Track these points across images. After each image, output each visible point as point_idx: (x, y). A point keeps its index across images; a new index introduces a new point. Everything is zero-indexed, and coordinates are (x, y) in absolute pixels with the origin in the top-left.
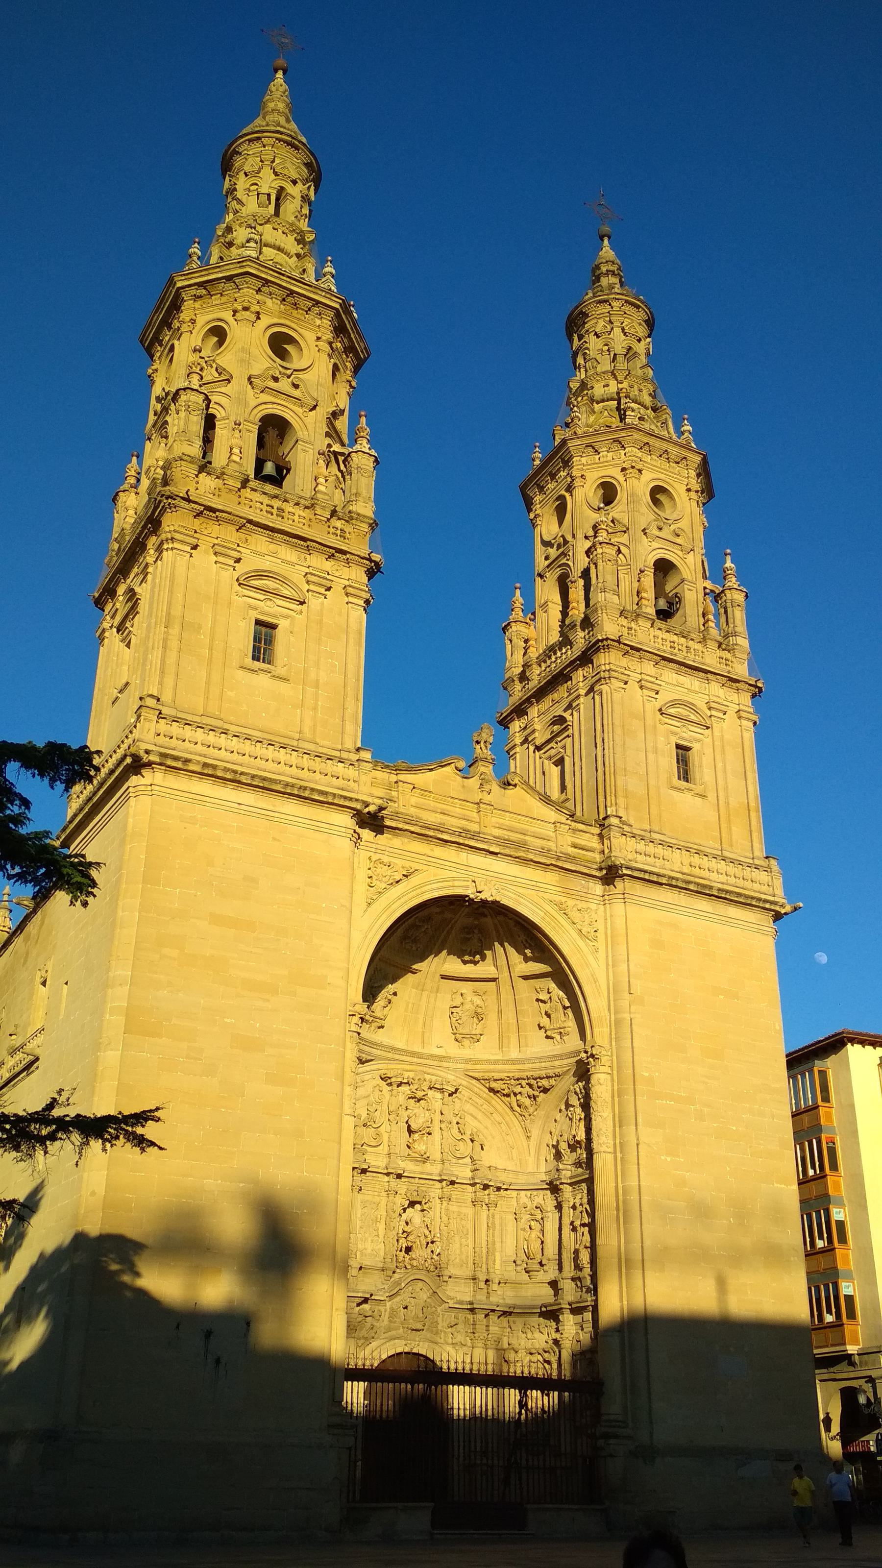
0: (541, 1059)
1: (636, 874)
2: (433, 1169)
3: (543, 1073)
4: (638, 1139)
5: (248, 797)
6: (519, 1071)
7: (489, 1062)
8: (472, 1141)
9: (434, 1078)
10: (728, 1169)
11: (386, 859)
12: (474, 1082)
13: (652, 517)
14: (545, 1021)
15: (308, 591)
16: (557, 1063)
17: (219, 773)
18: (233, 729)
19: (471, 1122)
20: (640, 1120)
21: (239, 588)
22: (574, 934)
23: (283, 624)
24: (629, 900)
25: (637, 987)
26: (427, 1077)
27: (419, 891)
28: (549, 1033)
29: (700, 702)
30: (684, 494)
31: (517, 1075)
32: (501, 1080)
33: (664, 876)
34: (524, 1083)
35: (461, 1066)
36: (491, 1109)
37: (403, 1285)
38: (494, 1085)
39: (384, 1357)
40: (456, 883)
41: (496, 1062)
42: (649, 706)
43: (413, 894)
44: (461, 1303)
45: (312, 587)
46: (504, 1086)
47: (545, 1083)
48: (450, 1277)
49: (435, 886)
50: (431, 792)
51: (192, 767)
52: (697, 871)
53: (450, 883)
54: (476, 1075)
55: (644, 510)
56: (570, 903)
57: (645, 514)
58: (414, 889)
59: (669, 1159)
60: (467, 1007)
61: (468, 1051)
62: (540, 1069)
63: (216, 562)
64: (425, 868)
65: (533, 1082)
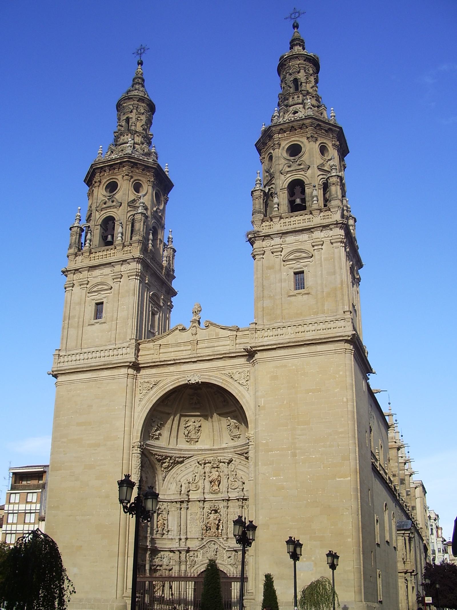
2: (220, 496)
9: (219, 458)
10: (309, 477)
11: (146, 380)
19: (240, 473)
24: (259, 362)
35: (233, 450)
37: (205, 543)
40: (180, 380)
50: (169, 344)
53: (177, 381)
54: (239, 452)
56: (234, 371)
58: (160, 388)
59: (274, 478)
60: (231, 424)
64: (165, 378)
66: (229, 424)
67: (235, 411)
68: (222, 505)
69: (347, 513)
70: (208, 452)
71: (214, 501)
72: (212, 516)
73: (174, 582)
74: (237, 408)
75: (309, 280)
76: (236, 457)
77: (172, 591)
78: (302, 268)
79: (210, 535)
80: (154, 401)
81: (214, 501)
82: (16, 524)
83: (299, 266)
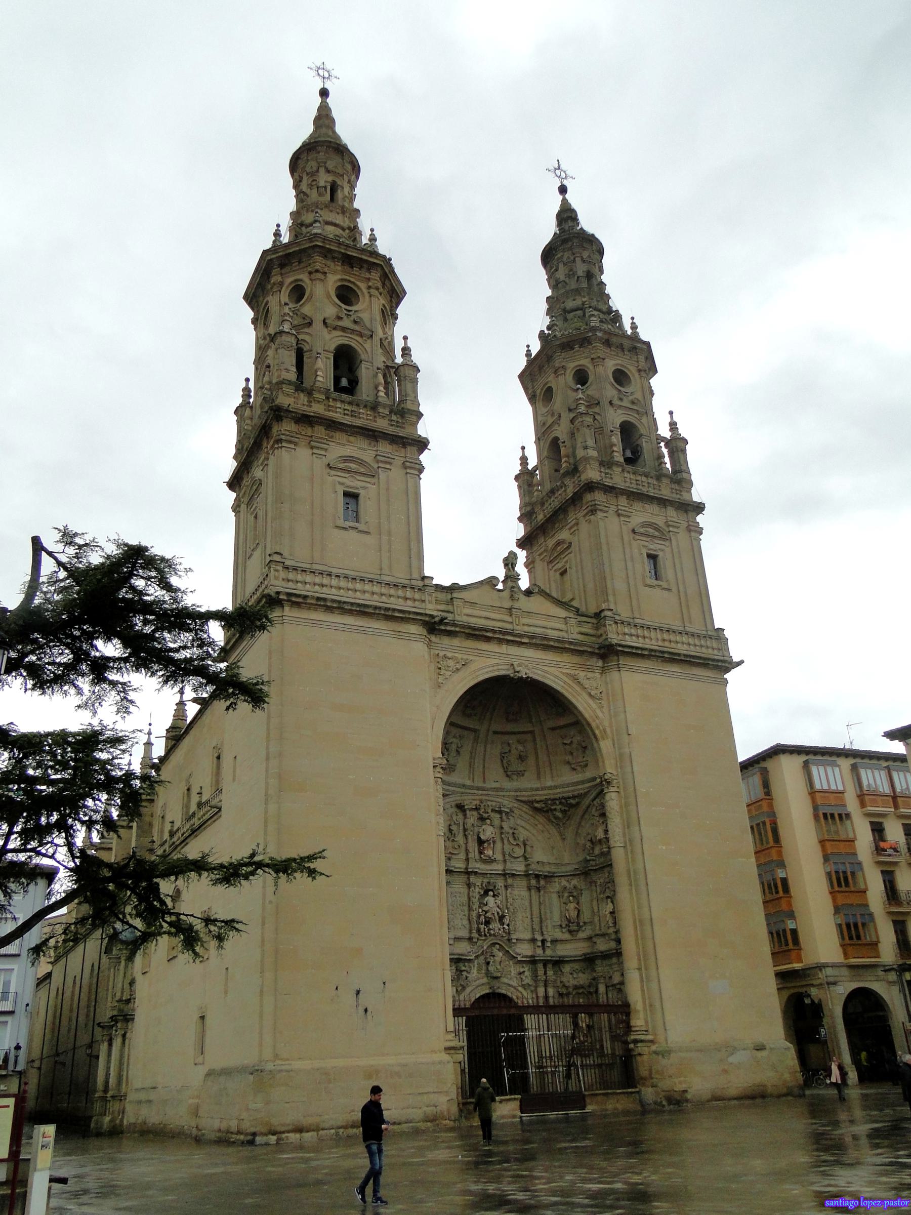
0: (568, 785)
1: (626, 650)
2: (498, 867)
3: (570, 794)
4: (641, 836)
5: (350, 620)
6: (554, 794)
7: (532, 790)
8: (525, 845)
9: (494, 804)
11: (449, 655)
12: (522, 804)
13: (615, 392)
14: (569, 758)
15: (378, 467)
16: (580, 787)
17: (329, 604)
18: (334, 571)
20: (642, 823)
21: (329, 470)
22: (586, 697)
23: (362, 493)
25: (633, 730)
26: (489, 803)
28: (573, 766)
29: (660, 521)
30: (637, 375)
31: (552, 797)
32: (541, 801)
33: (646, 649)
34: (557, 802)
36: (537, 823)
38: (536, 805)
41: (537, 789)
42: (624, 527)
44: (526, 957)
45: (381, 465)
46: (544, 805)
47: (573, 801)
48: (517, 940)
49: (486, 670)
51: (309, 601)
52: (667, 644)
53: (496, 668)
55: (609, 387)
57: (610, 392)
59: (664, 848)
60: (514, 751)
61: (515, 784)
62: (569, 792)
63: (313, 453)
65: (563, 801)
67: (532, 732)
68: (500, 883)
70: (472, 791)
71: (488, 875)
76: (516, 805)
79: (494, 935)
81: (488, 875)
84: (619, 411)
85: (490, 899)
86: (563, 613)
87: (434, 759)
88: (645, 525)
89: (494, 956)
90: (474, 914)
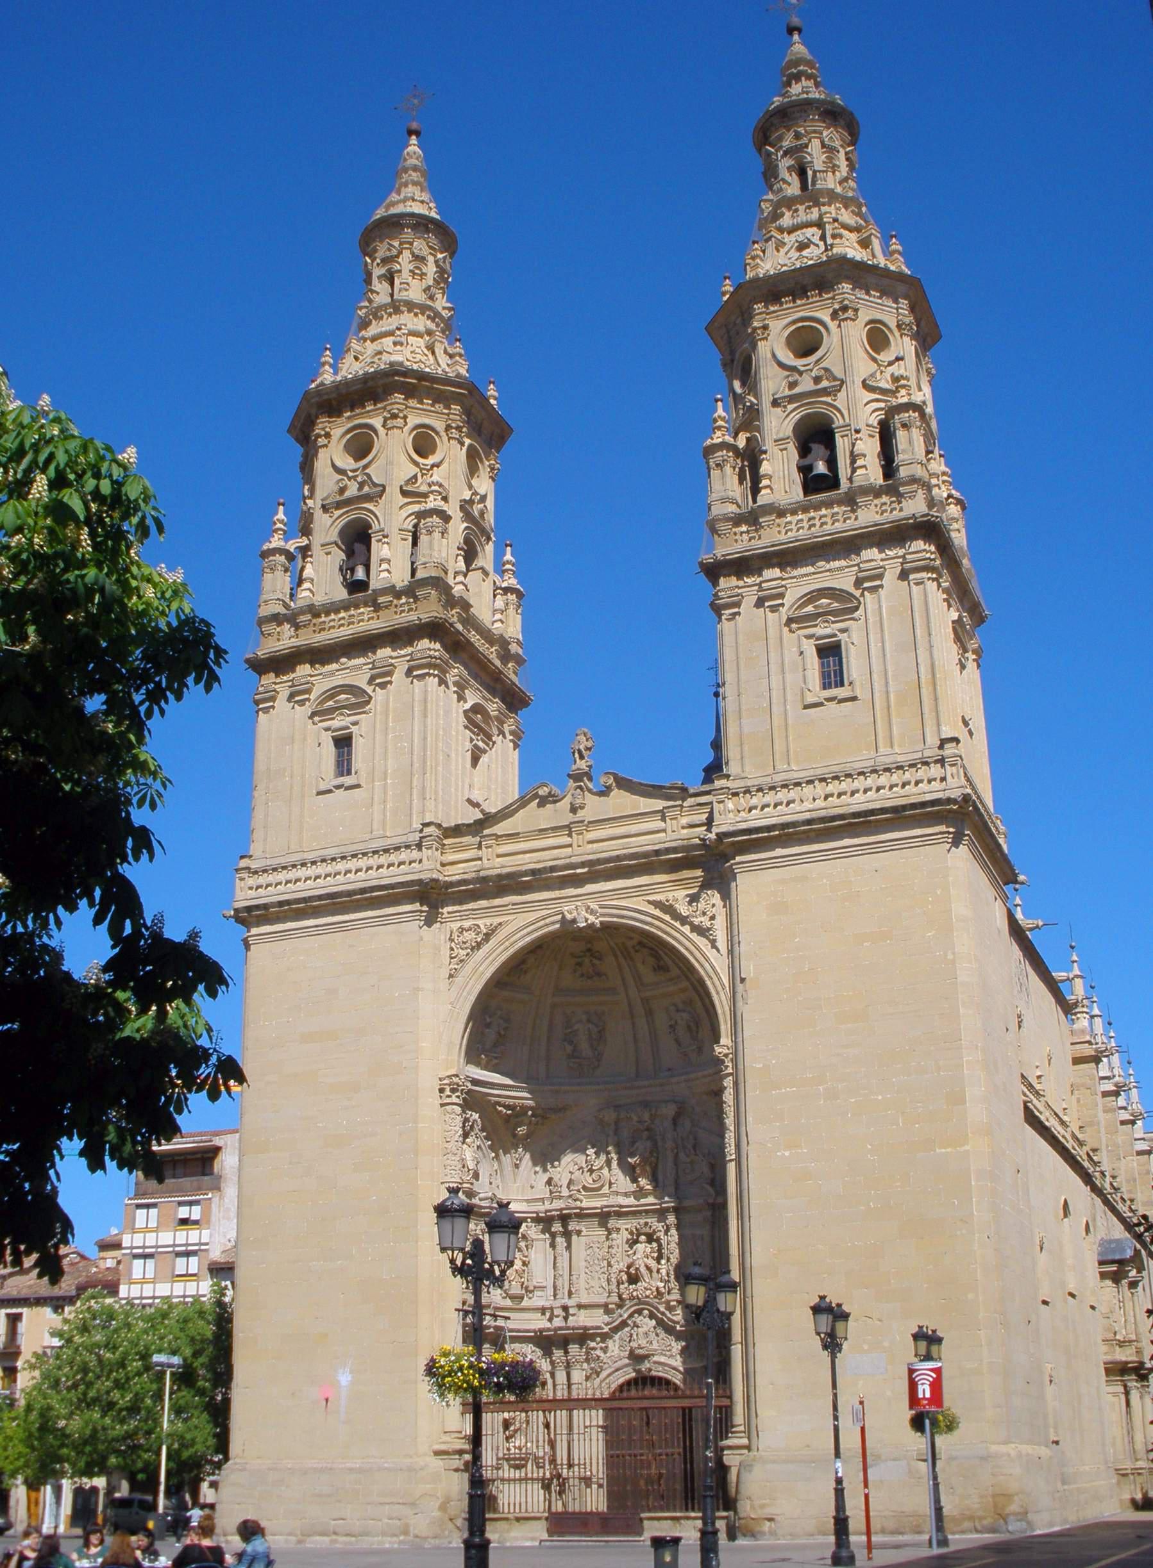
11: (466, 924)
18: (311, 856)
27: (507, 943)
37: (626, 1316)
39: (621, 1380)
40: (548, 921)
43: (502, 947)
49: (525, 931)
50: (518, 834)
58: (501, 943)
59: (787, 1154)
60: (679, 1022)
64: (511, 917)
66: (673, 1022)
69: (964, 1231)
72: (642, 1247)
73: (553, 1413)
74: (692, 984)
75: (854, 664)
77: (549, 1434)
78: (835, 635)
80: (488, 975)
82: (154, 1281)
83: (828, 631)
84: (790, 407)
85: (642, 1247)
86: (659, 804)
87: (440, 1079)
88: (812, 597)
89: (638, 1327)
90: (616, 1267)
